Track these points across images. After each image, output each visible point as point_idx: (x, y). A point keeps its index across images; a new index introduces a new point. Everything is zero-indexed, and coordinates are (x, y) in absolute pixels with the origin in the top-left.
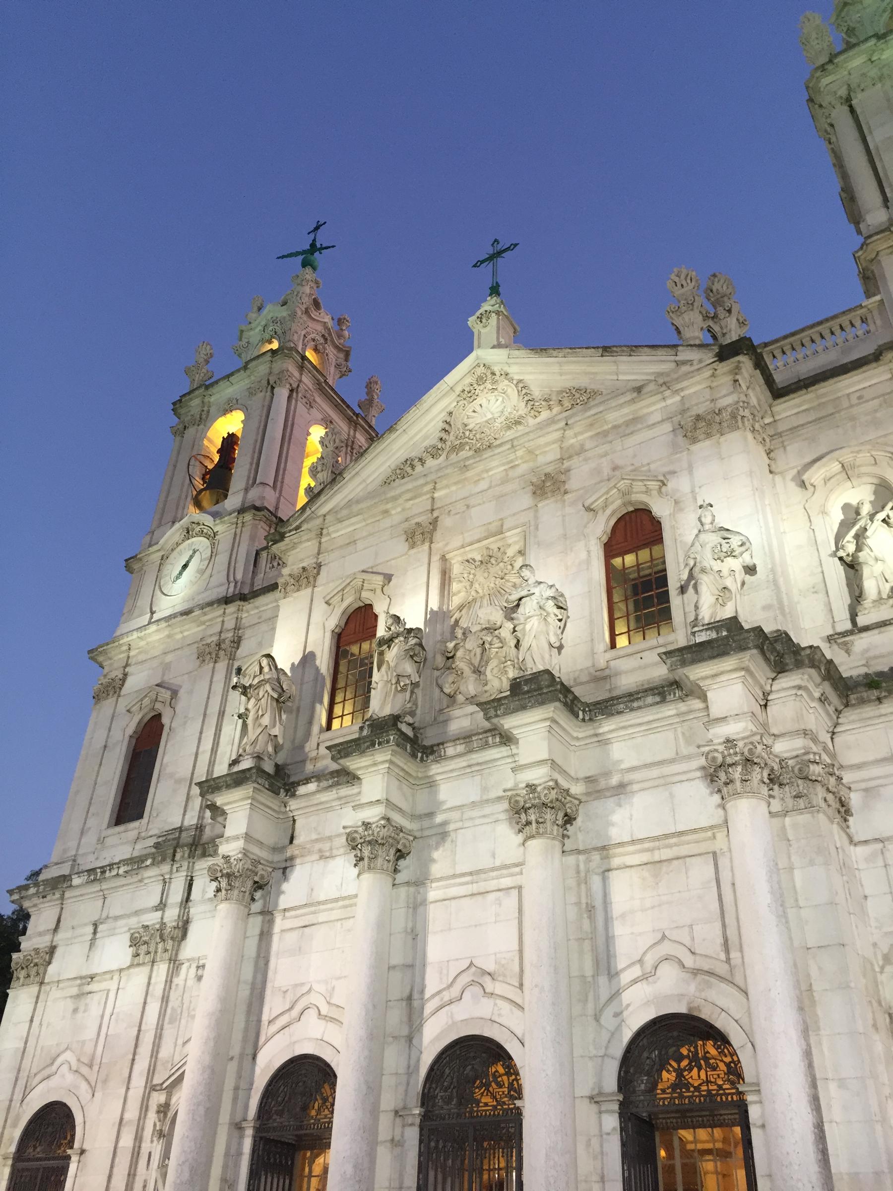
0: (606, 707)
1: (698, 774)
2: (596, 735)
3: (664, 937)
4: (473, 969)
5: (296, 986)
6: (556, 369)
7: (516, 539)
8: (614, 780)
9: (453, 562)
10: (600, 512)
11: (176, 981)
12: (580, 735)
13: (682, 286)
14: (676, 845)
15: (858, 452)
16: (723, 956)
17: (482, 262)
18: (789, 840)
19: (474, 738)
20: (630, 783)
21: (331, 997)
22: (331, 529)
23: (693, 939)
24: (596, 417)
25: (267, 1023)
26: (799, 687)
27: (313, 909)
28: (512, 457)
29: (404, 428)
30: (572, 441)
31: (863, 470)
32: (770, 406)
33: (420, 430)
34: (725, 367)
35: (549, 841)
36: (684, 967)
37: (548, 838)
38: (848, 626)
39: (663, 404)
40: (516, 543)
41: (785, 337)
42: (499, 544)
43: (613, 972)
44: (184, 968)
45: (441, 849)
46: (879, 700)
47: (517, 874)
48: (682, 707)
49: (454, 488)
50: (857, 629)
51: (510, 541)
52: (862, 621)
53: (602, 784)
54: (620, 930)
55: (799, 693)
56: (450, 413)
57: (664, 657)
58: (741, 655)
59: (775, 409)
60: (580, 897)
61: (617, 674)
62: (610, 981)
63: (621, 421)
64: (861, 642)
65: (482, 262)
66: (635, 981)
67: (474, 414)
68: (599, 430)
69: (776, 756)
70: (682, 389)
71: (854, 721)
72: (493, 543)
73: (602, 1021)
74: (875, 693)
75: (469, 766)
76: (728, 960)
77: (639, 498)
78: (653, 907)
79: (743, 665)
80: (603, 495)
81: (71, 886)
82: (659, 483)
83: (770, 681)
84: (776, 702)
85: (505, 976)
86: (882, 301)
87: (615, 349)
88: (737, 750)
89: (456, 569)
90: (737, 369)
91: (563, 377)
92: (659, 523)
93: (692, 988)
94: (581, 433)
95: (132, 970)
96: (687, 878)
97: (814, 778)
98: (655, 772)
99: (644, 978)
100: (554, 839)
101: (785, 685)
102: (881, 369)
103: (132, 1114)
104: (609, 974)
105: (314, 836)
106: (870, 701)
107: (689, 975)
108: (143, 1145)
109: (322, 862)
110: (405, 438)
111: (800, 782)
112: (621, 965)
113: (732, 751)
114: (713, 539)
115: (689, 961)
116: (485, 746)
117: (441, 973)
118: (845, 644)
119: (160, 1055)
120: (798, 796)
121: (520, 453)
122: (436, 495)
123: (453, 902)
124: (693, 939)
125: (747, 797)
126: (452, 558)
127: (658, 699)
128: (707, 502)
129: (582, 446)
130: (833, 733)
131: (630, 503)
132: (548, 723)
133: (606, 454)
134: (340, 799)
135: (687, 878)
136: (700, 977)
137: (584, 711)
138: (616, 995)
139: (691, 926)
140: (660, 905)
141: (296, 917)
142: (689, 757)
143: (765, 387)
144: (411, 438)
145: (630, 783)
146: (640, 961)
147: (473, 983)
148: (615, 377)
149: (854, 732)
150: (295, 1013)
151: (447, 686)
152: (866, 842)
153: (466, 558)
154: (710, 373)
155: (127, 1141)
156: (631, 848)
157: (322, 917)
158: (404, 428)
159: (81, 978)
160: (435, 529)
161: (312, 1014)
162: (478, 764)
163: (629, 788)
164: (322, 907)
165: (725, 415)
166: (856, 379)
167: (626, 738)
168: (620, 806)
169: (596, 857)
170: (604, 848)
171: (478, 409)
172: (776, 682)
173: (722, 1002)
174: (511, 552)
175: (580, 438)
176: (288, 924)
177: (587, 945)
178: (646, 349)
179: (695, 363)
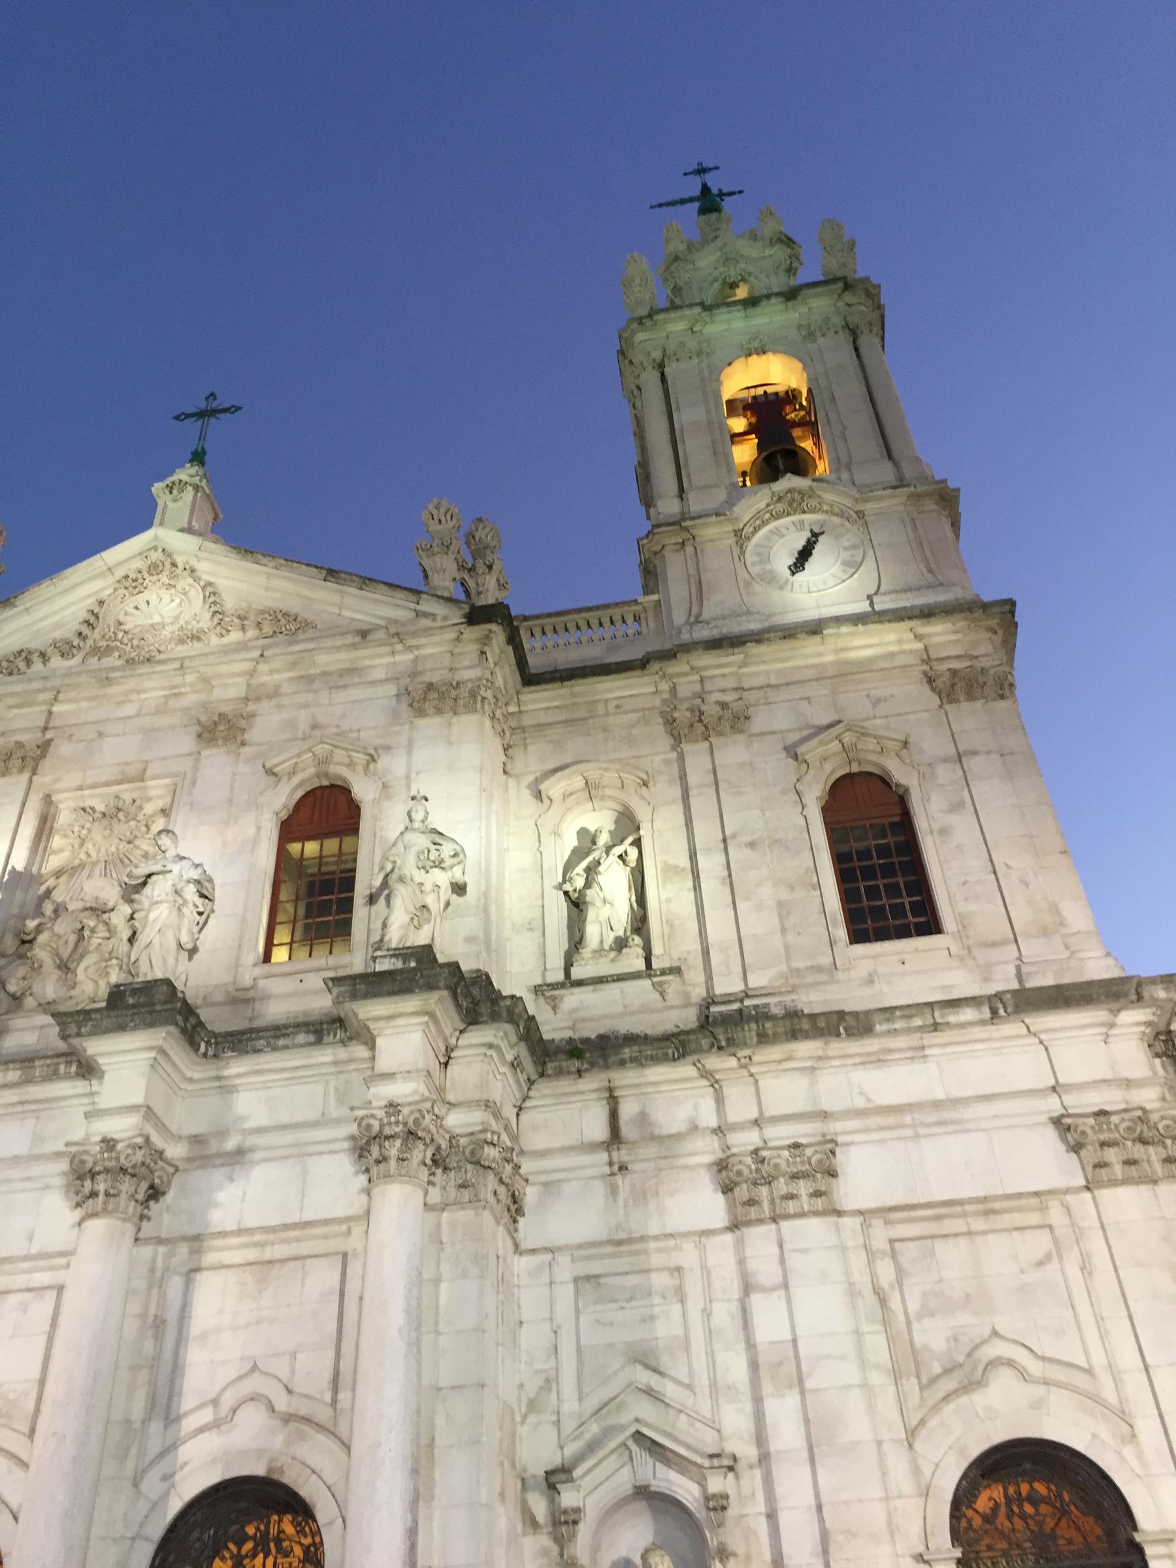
0: (240, 1041)
2: (219, 1078)
3: (255, 1368)
6: (262, 580)
7: (160, 792)
8: (231, 1144)
9: (61, 806)
10: (284, 780)
12: (196, 1076)
13: (440, 521)
14: (298, 1240)
15: (606, 770)
16: (328, 1397)
17: (188, 416)
18: (441, 1243)
19: (37, 1063)
20: (252, 1150)
23: (293, 1371)
24: (303, 654)
26: (490, 1046)
28: (178, 680)
29: (27, 605)
30: (265, 679)
31: (608, 792)
32: (518, 693)
33: (54, 613)
34: (473, 633)
35: (119, 1223)
36: (273, 1411)
37: (119, 1218)
38: (560, 976)
39: (390, 659)
40: (159, 797)
41: (550, 615)
42: (136, 795)
43: (173, 1416)
46: (579, 1073)
47: (60, 1267)
48: (342, 1053)
49: (84, 705)
50: (570, 982)
51: (152, 793)
52: (577, 973)
53: (213, 1147)
55: (490, 1052)
56: (101, 603)
57: (330, 984)
58: (426, 995)
59: (523, 698)
60: (146, 1306)
61: (265, 998)
62: (166, 1427)
63: (333, 668)
64: (572, 999)
65: (188, 416)
66: (201, 1430)
67: (135, 611)
68: (303, 673)
69: (447, 1131)
70: (418, 647)
71: (545, 1096)
72: (127, 792)
73: (144, 1487)
74: (575, 1064)
75: (22, 1103)
76: (335, 1401)
78: (248, 1325)
79: (428, 1009)
80: (291, 758)
82: (367, 757)
83: (457, 1033)
84: (460, 1060)
86: (659, 601)
87: (343, 575)
88: (401, 1118)
89: (64, 817)
90: (486, 640)
91: (269, 594)
92: (358, 808)
93: (278, 1441)
94: (279, 671)
96: (303, 1286)
97: (487, 1164)
98: (290, 1137)
99: (215, 1425)
100: (125, 1220)
101: (474, 1041)
102: (646, 679)
104: (166, 1419)
106: (569, 1073)
107: (278, 1422)
110: (26, 620)
111: (470, 1167)
112: (187, 1403)
113: (393, 1119)
114: (421, 841)
115: (282, 1403)
116: (53, 1076)
118: (554, 998)
120: (463, 1186)
121: (190, 678)
122: (55, 709)
124: (293, 1371)
125: (401, 1182)
126: (60, 802)
127: (312, 1038)
128: (422, 793)
129: (277, 687)
130: (520, 1108)
131: (326, 775)
132: (153, 1054)
133: (306, 706)
135: (303, 1286)
136: (292, 1426)
137: (208, 1043)
138: (169, 1449)
139: (294, 1354)
140: (258, 1323)
142: (337, 1122)
143: (515, 668)
144: (38, 621)
145: (252, 1150)
146: (215, 1402)
148: (337, 611)
149: (543, 1109)
151: (13, 981)
152: (533, 1251)
153: (81, 804)
154: (453, 635)
156: (234, 1241)
158: (27, 605)
160: (43, 756)
162: (36, 1101)
163: (249, 1156)
165: (464, 692)
166: (617, 684)
167: (259, 1086)
168: (231, 1179)
169: (183, 1250)
170: (197, 1238)
171: (143, 606)
172: (465, 1035)
173: (314, 1460)
174: (149, 808)
175: (276, 677)
177: (144, 1376)
178: (382, 585)
179: (438, 618)
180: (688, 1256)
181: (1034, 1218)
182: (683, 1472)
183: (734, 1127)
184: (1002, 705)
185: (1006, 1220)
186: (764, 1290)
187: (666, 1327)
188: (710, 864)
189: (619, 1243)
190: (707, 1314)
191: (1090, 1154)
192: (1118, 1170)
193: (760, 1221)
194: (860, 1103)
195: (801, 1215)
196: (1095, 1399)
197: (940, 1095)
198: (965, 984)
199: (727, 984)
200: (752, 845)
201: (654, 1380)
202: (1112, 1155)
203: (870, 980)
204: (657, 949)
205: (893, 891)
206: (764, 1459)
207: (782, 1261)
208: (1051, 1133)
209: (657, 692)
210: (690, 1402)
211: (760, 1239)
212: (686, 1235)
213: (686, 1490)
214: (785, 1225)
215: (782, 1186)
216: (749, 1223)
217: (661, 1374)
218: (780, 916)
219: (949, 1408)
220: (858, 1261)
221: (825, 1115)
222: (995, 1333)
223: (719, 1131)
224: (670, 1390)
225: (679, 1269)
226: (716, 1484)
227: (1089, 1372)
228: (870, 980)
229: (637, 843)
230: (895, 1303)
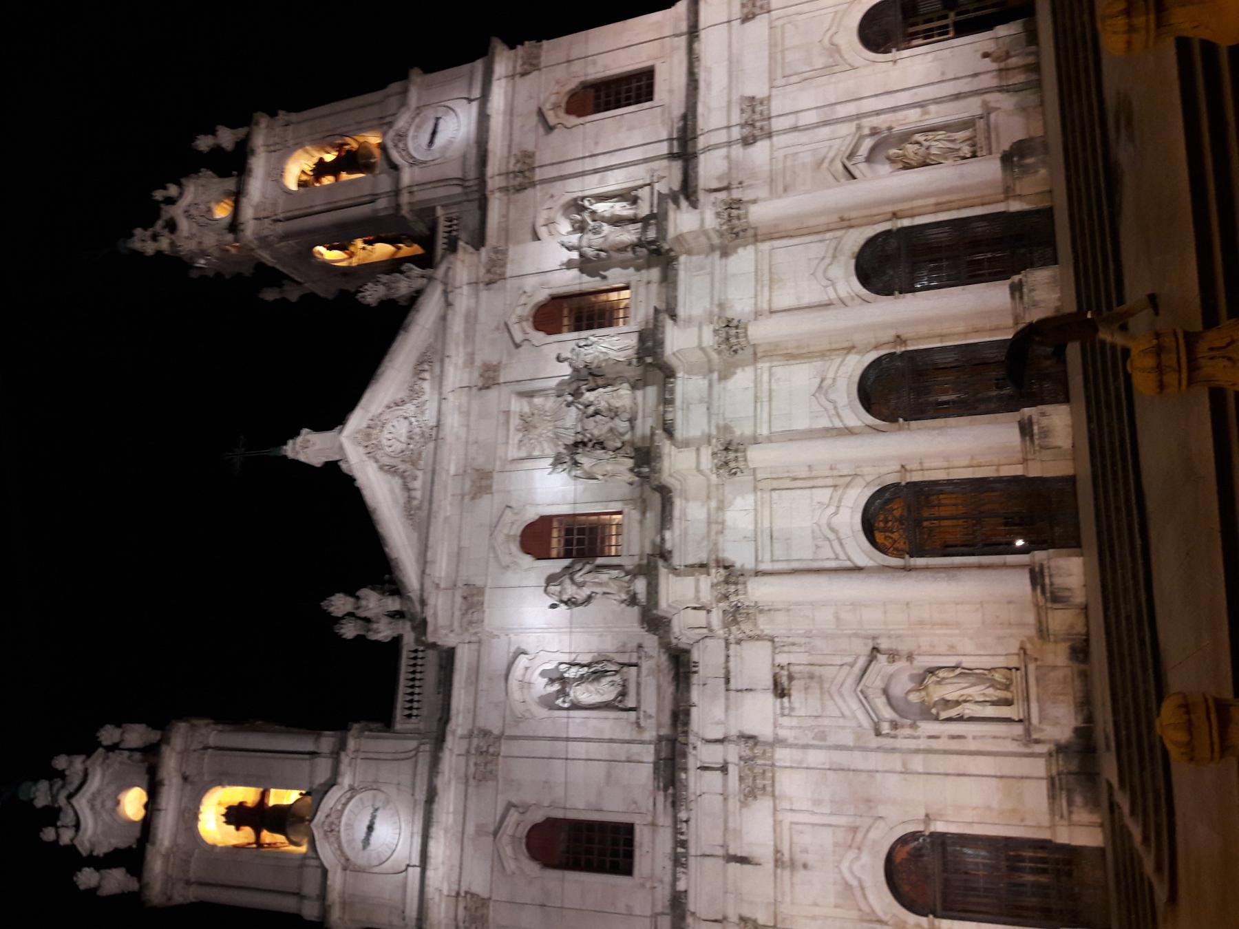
1: (724, 260)
4: (817, 394)
5: (814, 538)
8: (716, 310)
11: (791, 741)
21: (823, 504)
22: (437, 575)
23: (817, 258)
25: (838, 562)
27: (759, 534)
42: (517, 416)
44: (783, 733)
45: (735, 429)
54: (806, 300)
66: (835, 290)
72: (515, 422)
81: (686, 891)
85: (823, 371)
89: (523, 454)
93: (842, 259)
95: (777, 793)
98: (717, 285)
99: (833, 285)
103: (896, 762)
105: (705, 543)
108: (922, 747)
109: (727, 532)
115: (828, 261)
116: (672, 391)
117: (817, 417)
119: (851, 744)
123: (774, 413)
134: (680, 519)
139: (810, 259)
141: (763, 549)
145: (719, 299)
147: (826, 394)
150: (832, 536)
155: (917, 763)
156: (759, 298)
157: (767, 524)
159: (776, 866)
161: (836, 521)
164: (759, 525)
171: (390, 443)
176: (767, 556)
180: (780, 154)
181: (779, 31)
182: (861, 145)
183: (729, 136)
186: (797, 121)
187: (807, 158)
188: (602, 162)
189: (772, 180)
191: (757, 11)
193: (770, 125)
194: (725, 91)
195: (769, 109)
197: (726, 63)
198: (680, 59)
199: (664, 149)
200: (596, 144)
201: (827, 161)
203: (671, 91)
204: (640, 183)
205: (628, 91)
206: (859, 116)
208: (747, 24)
209: (500, 199)
210: (836, 147)
211: (777, 124)
212: (771, 154)
213: (868, 144)
215: (757, 117)
217: (823, 160)
219: (846, 57)
220: (789, 88)
221: (729, 103)
222: (820, 41)
224: (831, 154)
226: (866, 131)
227: (836, 12)
228: (671, 91)
229: (583, 198)
230: (806, 75)
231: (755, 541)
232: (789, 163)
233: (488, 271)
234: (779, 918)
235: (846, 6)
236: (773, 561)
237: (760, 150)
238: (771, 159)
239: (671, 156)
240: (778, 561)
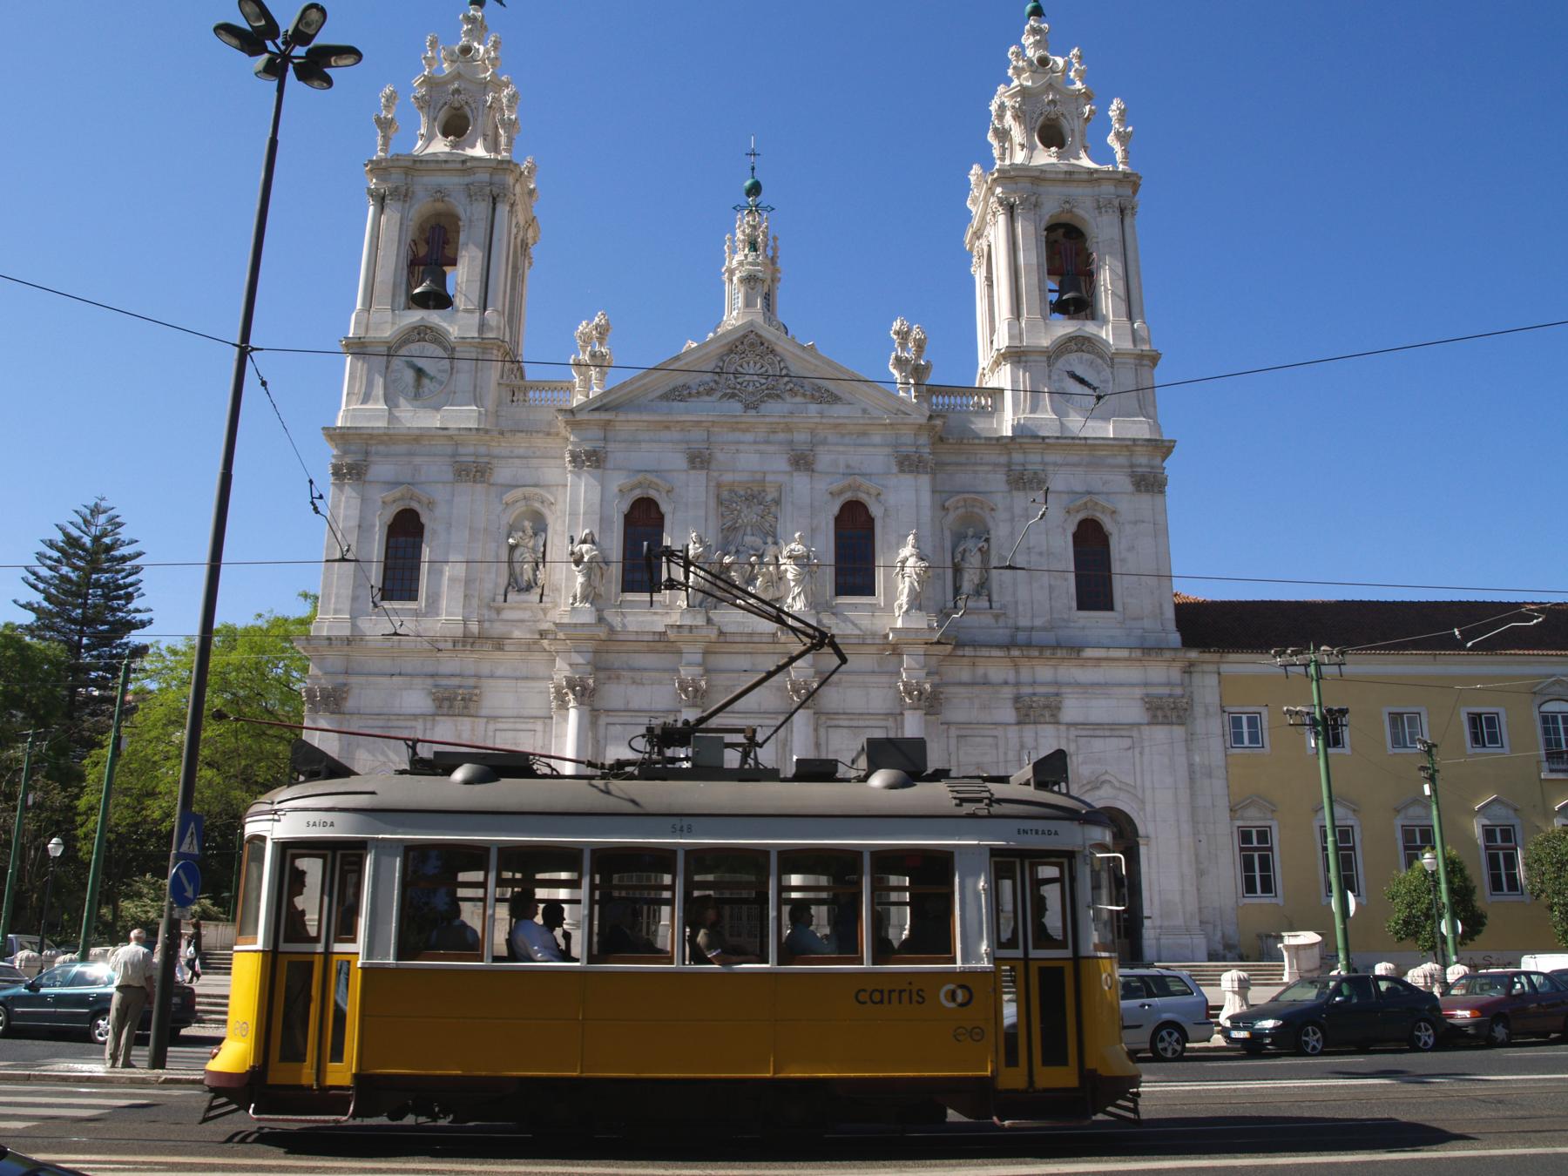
77: (863, 497)
95: (437, 718)
109: (634, 687)
174: (769, 498)
184: (1158, 497)
185: (1117, 733)
190: (1006, 754)
192: (1160, 719)
196: (1136, 796)
197: (1102, 680)
199: (1024, 622)
200: (1041, 554)
202: (1159, 713)
204: (995, 597)
207: (1036, 740)
214: (1039, 726)
216: (1025, 723)
218: (1050, 593)
221: (1056, 683)
222: (1106, 772)
223: (1017, 684)
225: (996, 737)
227: (1135, 787)
231: (625, 711)
232: (990, 740)
233: (907, 457)
234: (348, 717)
235: (1140, 794)
236: (608, 724)
237: (1009, 714)
238: (995, 724)
239: (1017, 629)
240: (606, 729)
